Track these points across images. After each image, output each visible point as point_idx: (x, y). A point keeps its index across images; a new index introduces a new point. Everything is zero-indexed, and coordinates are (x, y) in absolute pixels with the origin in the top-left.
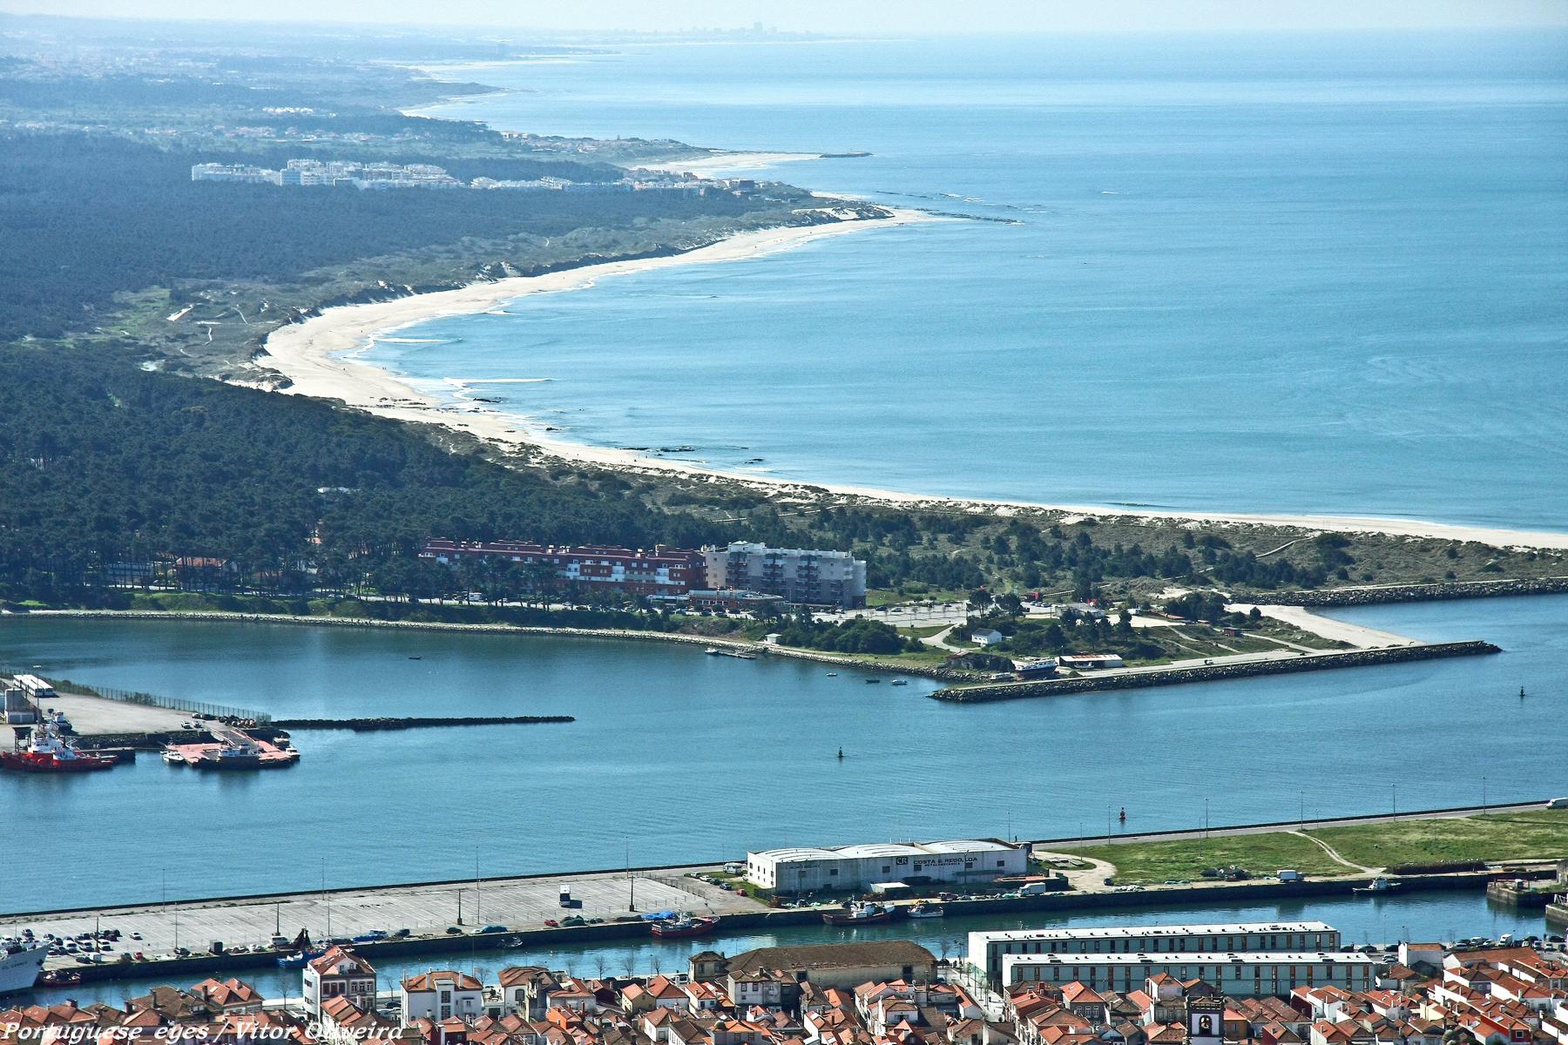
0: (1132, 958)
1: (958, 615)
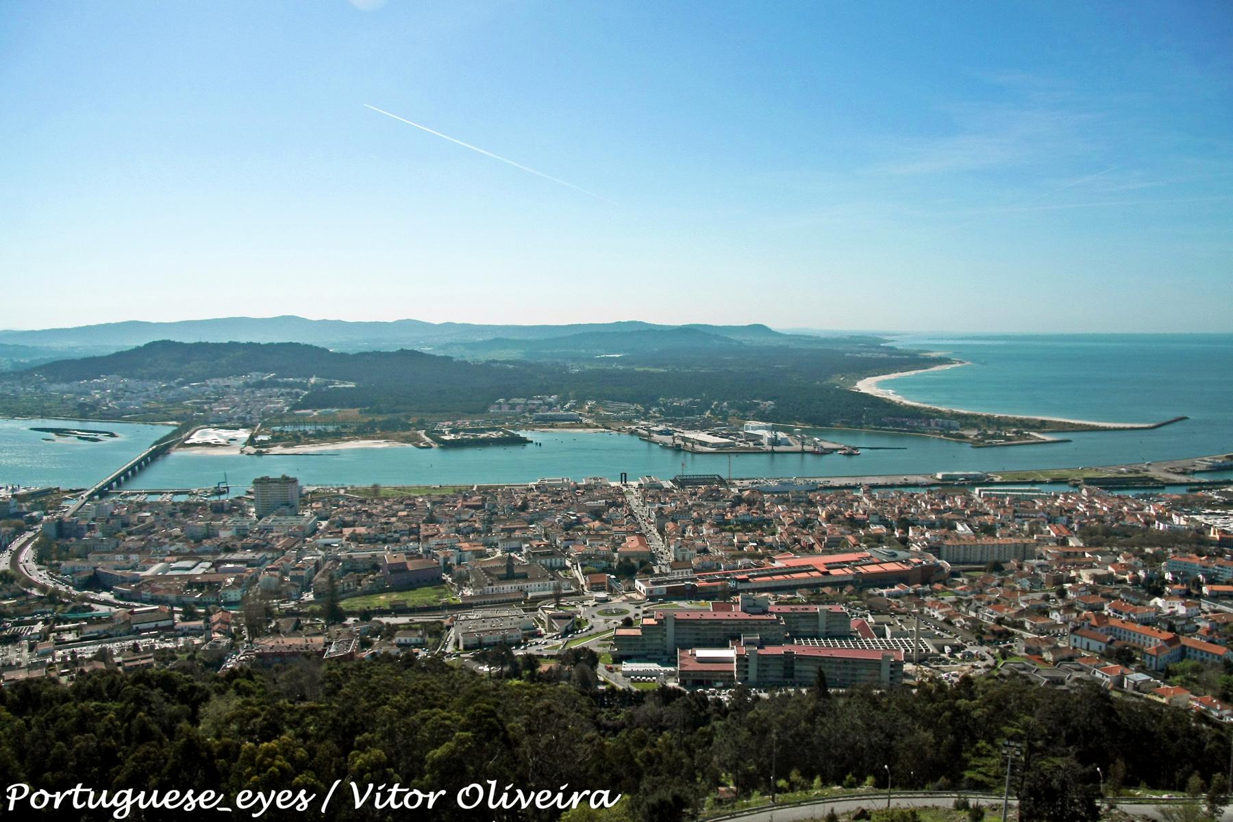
1: (975, 432)
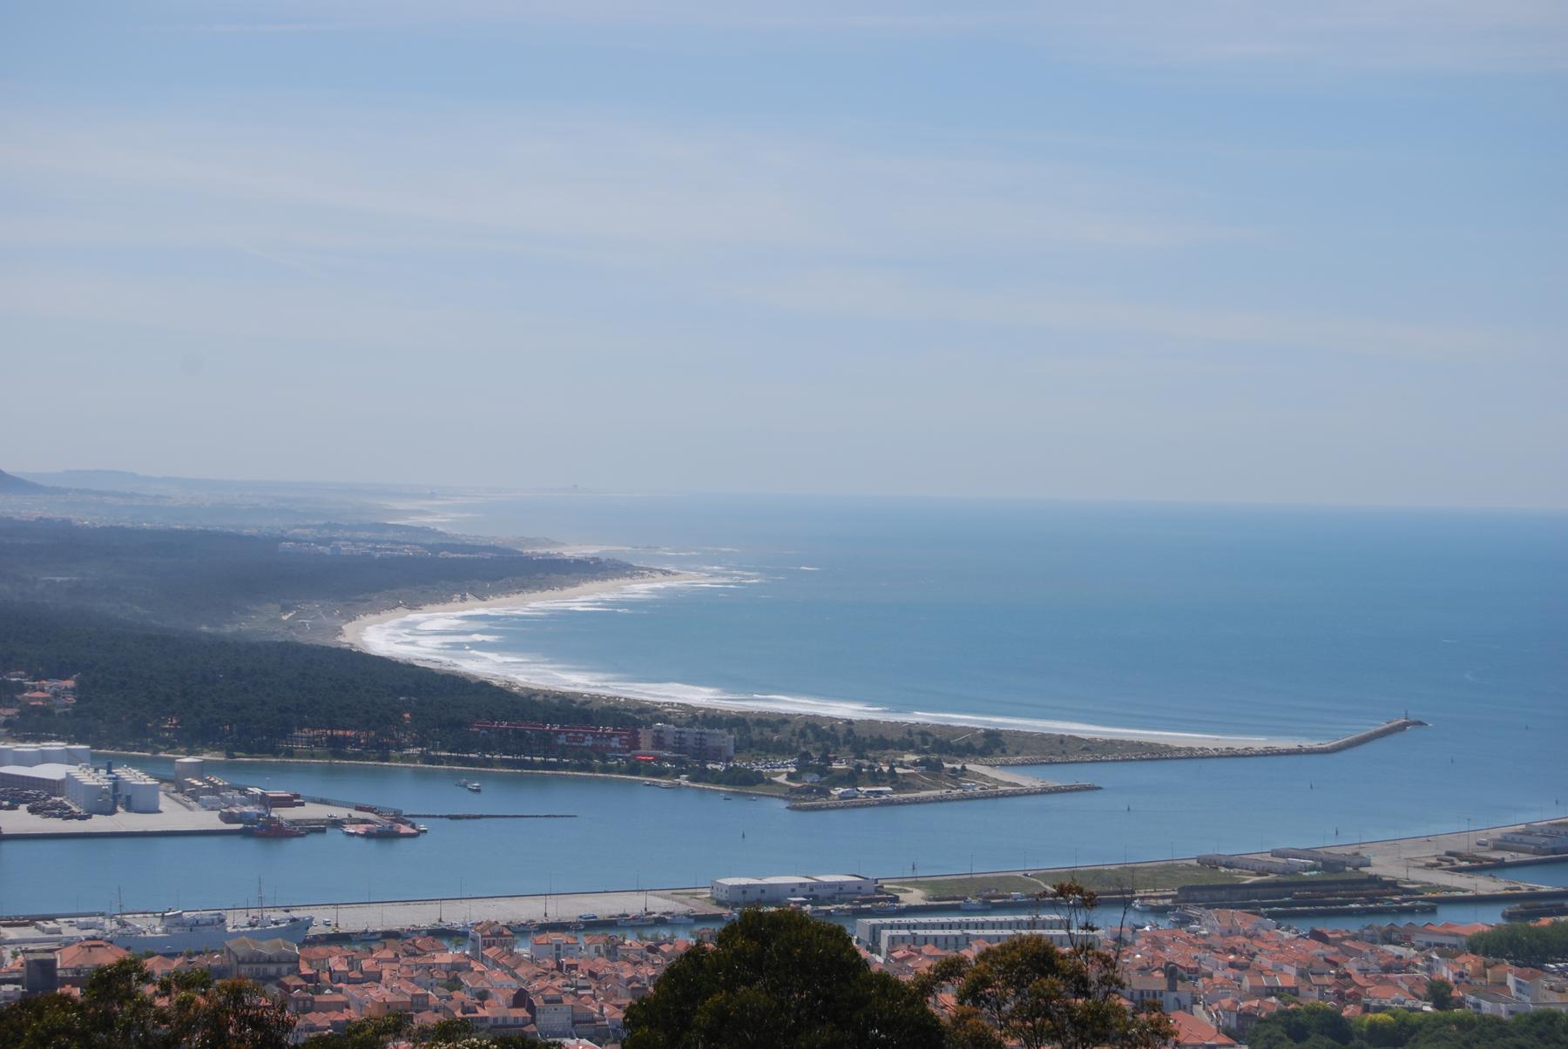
0: (957, 932)
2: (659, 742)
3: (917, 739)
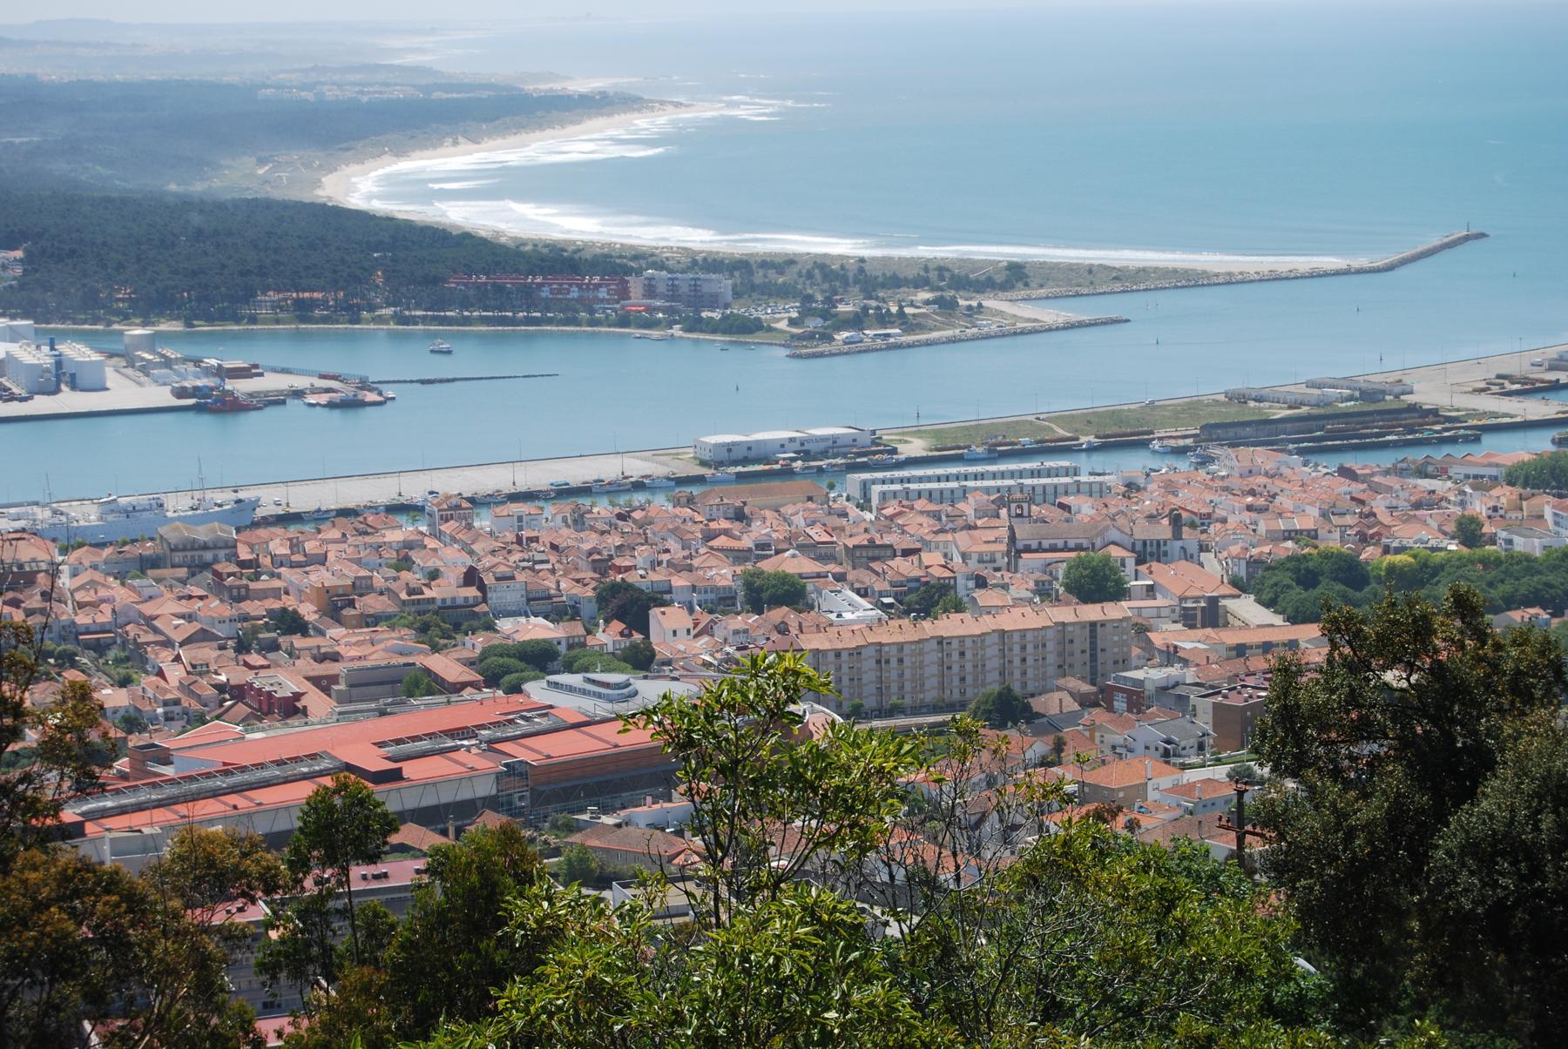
0: (953, 485)
2: (650, 291)
3: (933, 275)
